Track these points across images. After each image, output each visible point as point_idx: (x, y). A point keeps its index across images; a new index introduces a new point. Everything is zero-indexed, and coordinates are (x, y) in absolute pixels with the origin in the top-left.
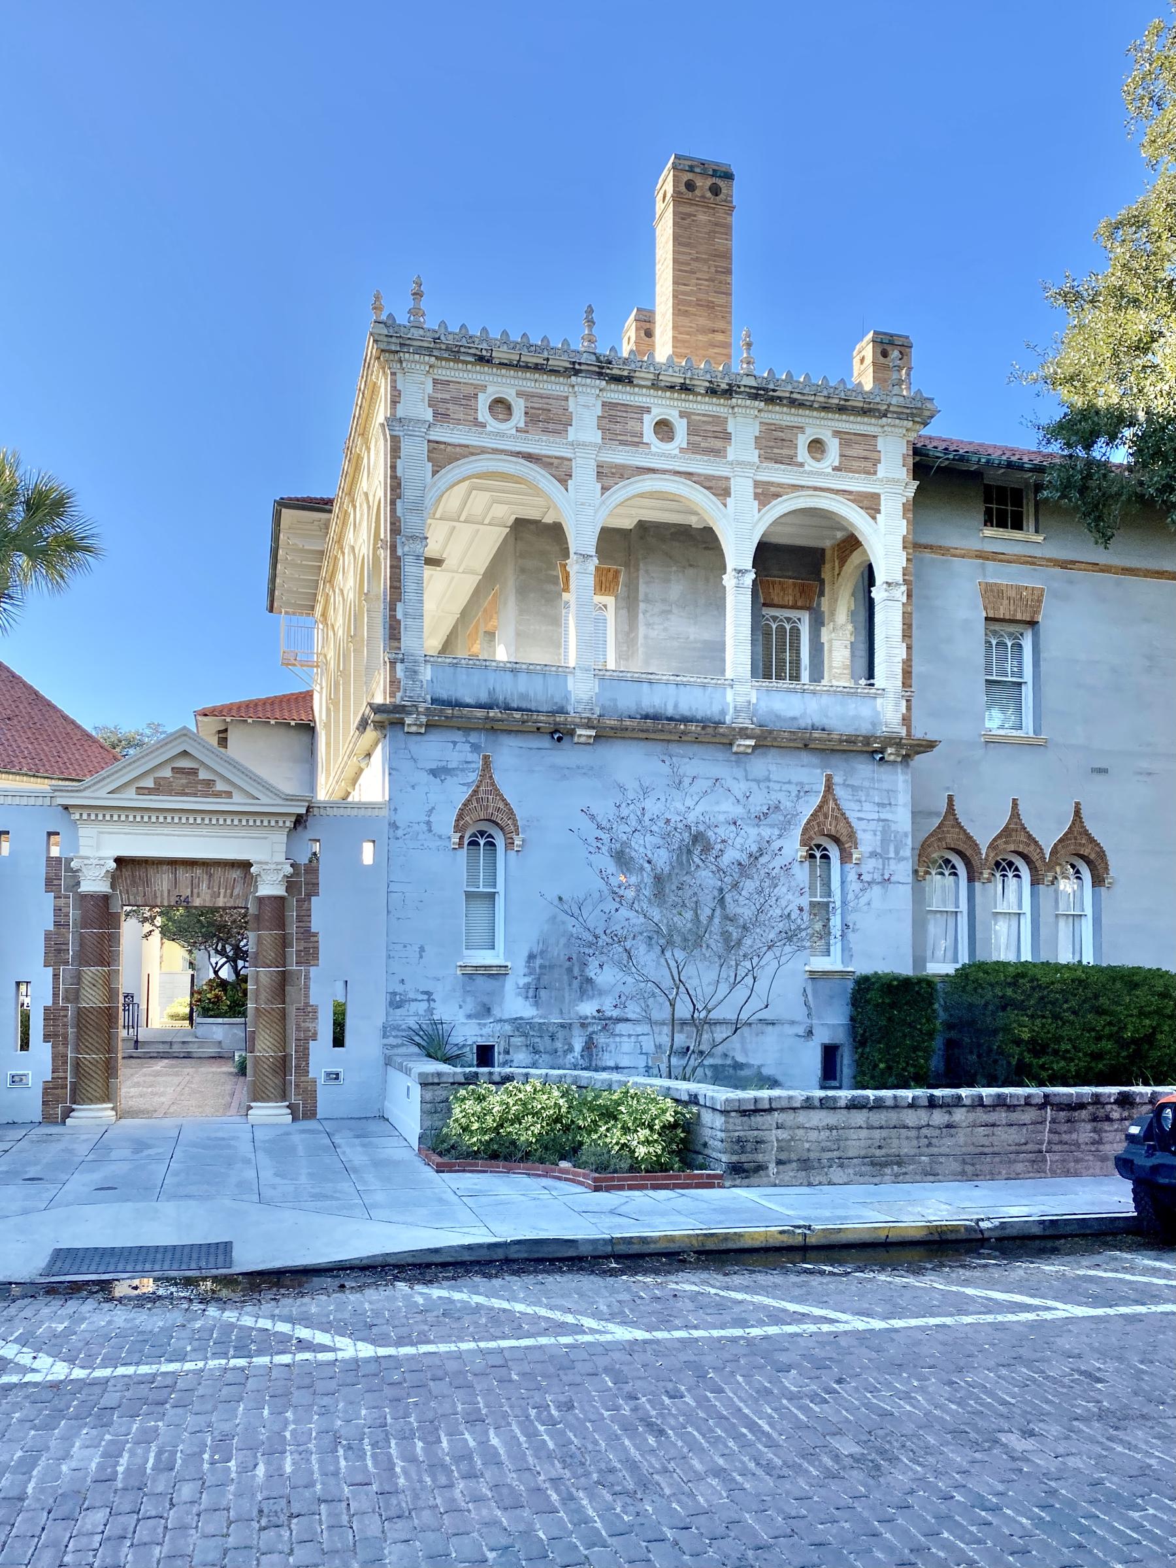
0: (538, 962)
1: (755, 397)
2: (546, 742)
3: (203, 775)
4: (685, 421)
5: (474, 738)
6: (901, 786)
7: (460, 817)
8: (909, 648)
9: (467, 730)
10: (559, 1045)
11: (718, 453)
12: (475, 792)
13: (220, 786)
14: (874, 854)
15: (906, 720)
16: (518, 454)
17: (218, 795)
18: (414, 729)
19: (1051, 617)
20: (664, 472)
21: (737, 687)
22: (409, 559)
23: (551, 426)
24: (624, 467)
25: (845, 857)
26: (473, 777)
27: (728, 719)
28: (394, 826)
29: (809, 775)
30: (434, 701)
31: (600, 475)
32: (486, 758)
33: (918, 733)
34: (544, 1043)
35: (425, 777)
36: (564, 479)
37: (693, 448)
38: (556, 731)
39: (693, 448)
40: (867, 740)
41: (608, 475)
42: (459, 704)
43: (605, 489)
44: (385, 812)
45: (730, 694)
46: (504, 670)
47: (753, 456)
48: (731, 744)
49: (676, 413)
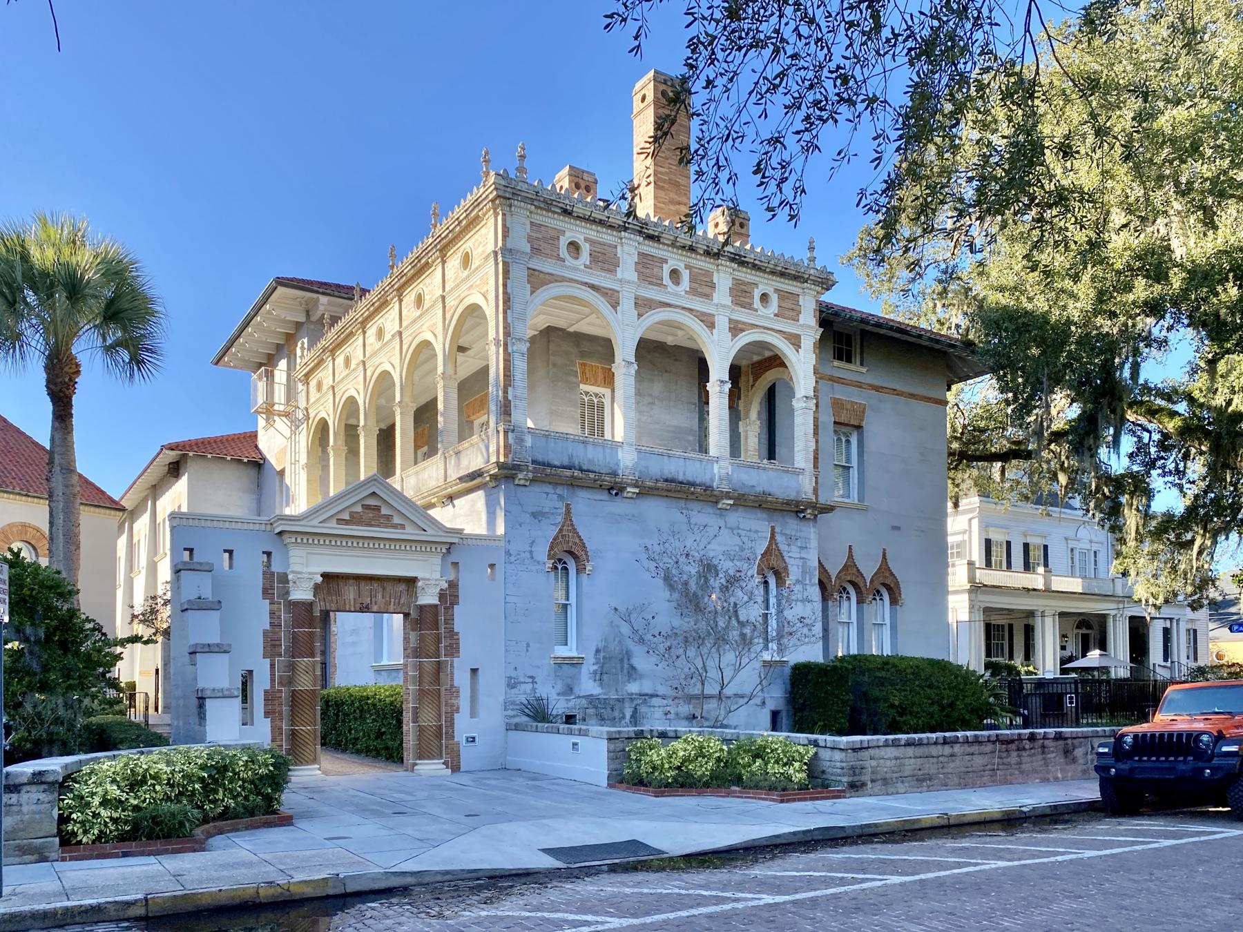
0: (602, 654)
1: (733, 260)
2: (605, 496)
3: (384, 511)
4: (688, 271)
5: (559, 491)
6: (812, 536)
7: (551, 548)
8: (817, 442)
9: (556, 484)
10: (616, 714)
11: (708, 296)
12: (561, 530)
13: (396, 520)
14: (798, 581)
15: (815, 491)
18: (522, 482)
19: (874, 427)
20: (676, 307)
21: (722, 463)
24: (651, 301)
25: (780, 581)
26: (559, 519)
27: (715, 485)
28: (508, 553)
30: (534, 462)
32: (568, 505)
33: (822, 500)
34: (606, 713)
35: (527, 518)
37: (693, 292)
38: (612, 488)
39: (693, 292)
40: (798, 503)
41: (643, 306)
43: (640, 315)
44: (502, 543)
46: (578, 441)
47: (728, 301)
48: (717, 503)
49: (683, 266)
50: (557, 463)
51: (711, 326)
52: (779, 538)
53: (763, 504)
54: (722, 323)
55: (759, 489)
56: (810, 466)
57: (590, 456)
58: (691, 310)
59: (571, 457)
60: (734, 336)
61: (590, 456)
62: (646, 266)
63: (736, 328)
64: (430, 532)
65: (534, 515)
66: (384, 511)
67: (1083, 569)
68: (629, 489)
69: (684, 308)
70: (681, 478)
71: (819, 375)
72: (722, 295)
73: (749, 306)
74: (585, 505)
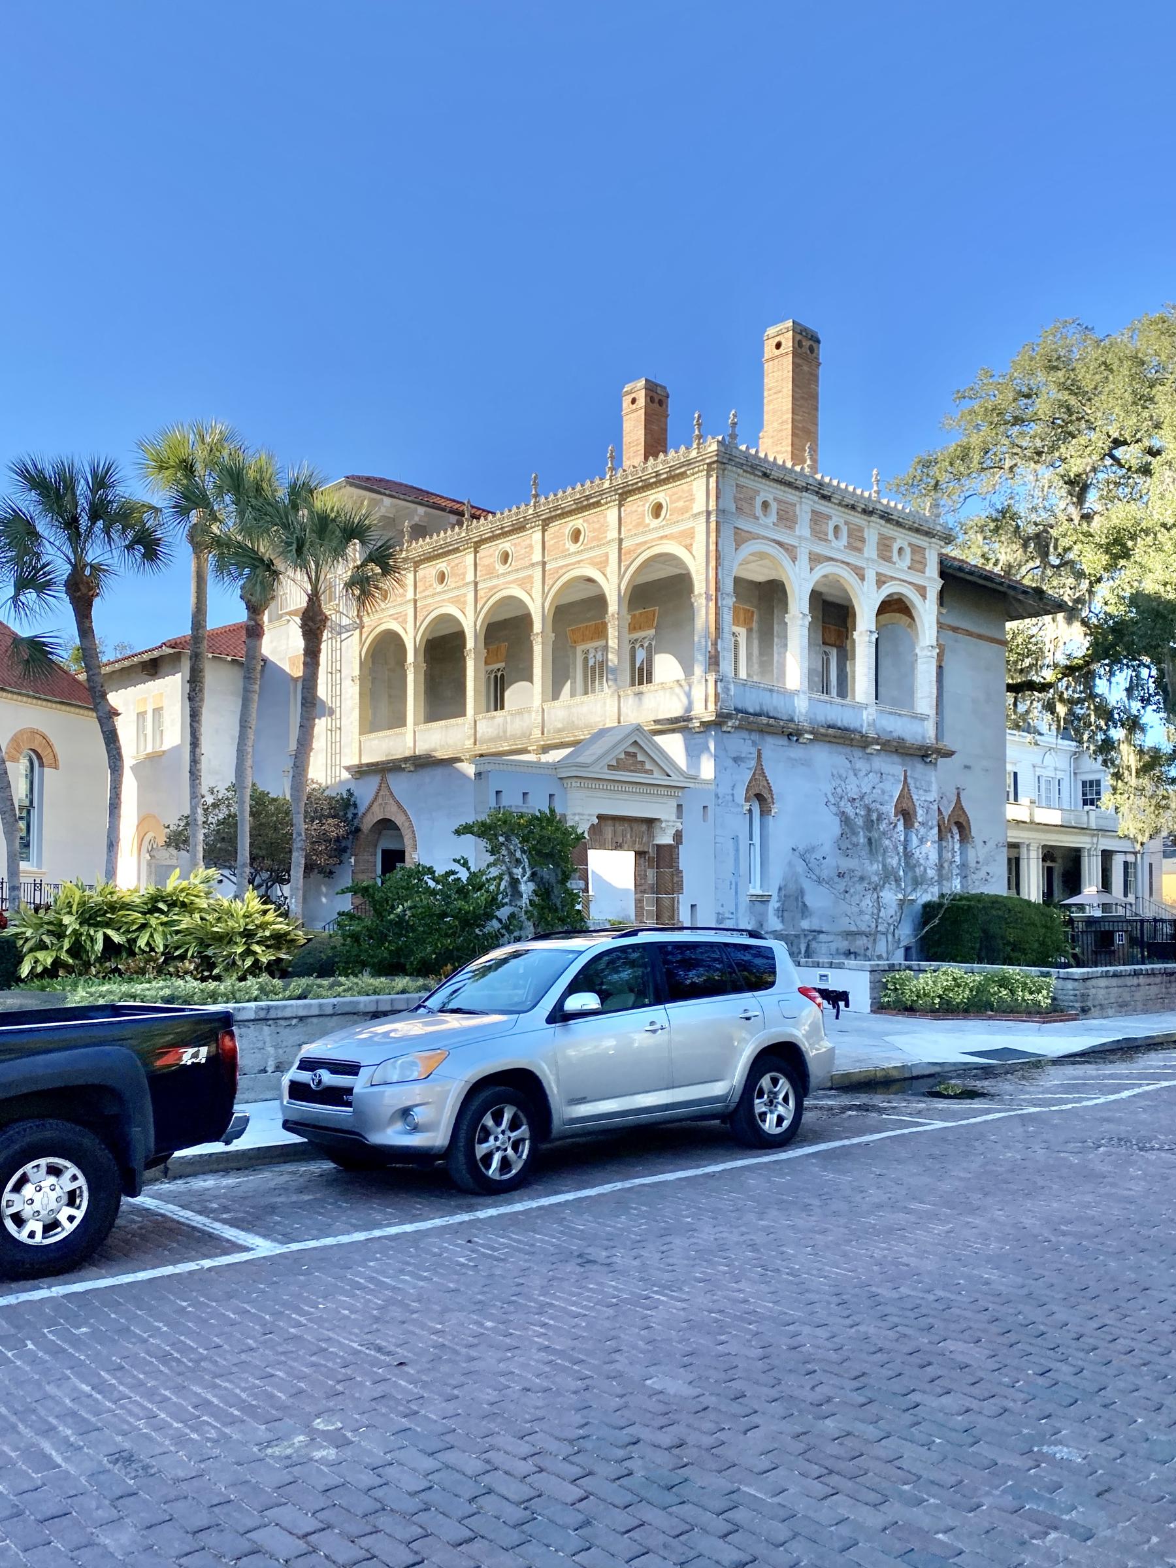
3: (640, 758)
9: (750, 731)
13: (648, 766)
16: (774, 541)
17: (646, 772)
22: (726, 609)
23: (788, 524)
26: (753, 764)
28: (717, 796)
29: (894, 768)
30: (735, 709)
31: (810, 560)
35: (730, 763)
36: (794, 559)
37: (850, 546)
39: (850, 546)
41: (816, 559)
42: (746, 713)
43: (811, 569)
44: (713, 787)
45: (865, 713)
50: (751, 711)
51: (862, 578)
52: (909, 780)
53: (897, 748)
54: (871, 576)
55: (895, 735)
56: (932, 712)
57: (775, 702)
58: (848, 564)
59: (761, 705)
60: (879, 588)
61: (773, 704)
62: (817, 518)
63: (881, 581)
64: (674, 777)
65: (736, 760)
66: (640, 758)
67: (1048, 798)
68: (807, 736)
69: (843, 562)
70: (839, 724)
71: (941, 626)
72: (870, 550)
73: (888, 559)
74: (772, 748)
